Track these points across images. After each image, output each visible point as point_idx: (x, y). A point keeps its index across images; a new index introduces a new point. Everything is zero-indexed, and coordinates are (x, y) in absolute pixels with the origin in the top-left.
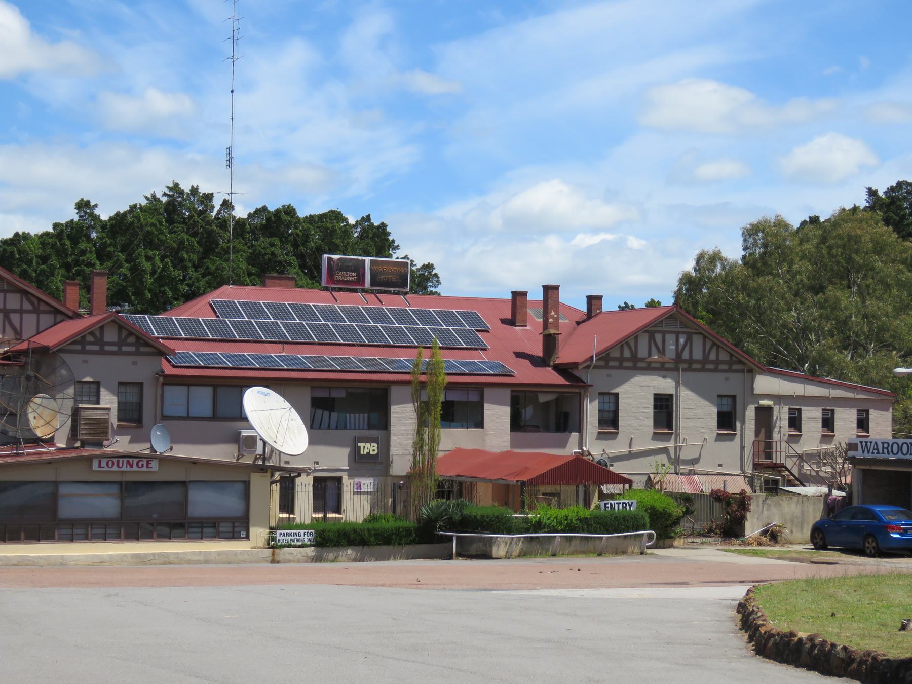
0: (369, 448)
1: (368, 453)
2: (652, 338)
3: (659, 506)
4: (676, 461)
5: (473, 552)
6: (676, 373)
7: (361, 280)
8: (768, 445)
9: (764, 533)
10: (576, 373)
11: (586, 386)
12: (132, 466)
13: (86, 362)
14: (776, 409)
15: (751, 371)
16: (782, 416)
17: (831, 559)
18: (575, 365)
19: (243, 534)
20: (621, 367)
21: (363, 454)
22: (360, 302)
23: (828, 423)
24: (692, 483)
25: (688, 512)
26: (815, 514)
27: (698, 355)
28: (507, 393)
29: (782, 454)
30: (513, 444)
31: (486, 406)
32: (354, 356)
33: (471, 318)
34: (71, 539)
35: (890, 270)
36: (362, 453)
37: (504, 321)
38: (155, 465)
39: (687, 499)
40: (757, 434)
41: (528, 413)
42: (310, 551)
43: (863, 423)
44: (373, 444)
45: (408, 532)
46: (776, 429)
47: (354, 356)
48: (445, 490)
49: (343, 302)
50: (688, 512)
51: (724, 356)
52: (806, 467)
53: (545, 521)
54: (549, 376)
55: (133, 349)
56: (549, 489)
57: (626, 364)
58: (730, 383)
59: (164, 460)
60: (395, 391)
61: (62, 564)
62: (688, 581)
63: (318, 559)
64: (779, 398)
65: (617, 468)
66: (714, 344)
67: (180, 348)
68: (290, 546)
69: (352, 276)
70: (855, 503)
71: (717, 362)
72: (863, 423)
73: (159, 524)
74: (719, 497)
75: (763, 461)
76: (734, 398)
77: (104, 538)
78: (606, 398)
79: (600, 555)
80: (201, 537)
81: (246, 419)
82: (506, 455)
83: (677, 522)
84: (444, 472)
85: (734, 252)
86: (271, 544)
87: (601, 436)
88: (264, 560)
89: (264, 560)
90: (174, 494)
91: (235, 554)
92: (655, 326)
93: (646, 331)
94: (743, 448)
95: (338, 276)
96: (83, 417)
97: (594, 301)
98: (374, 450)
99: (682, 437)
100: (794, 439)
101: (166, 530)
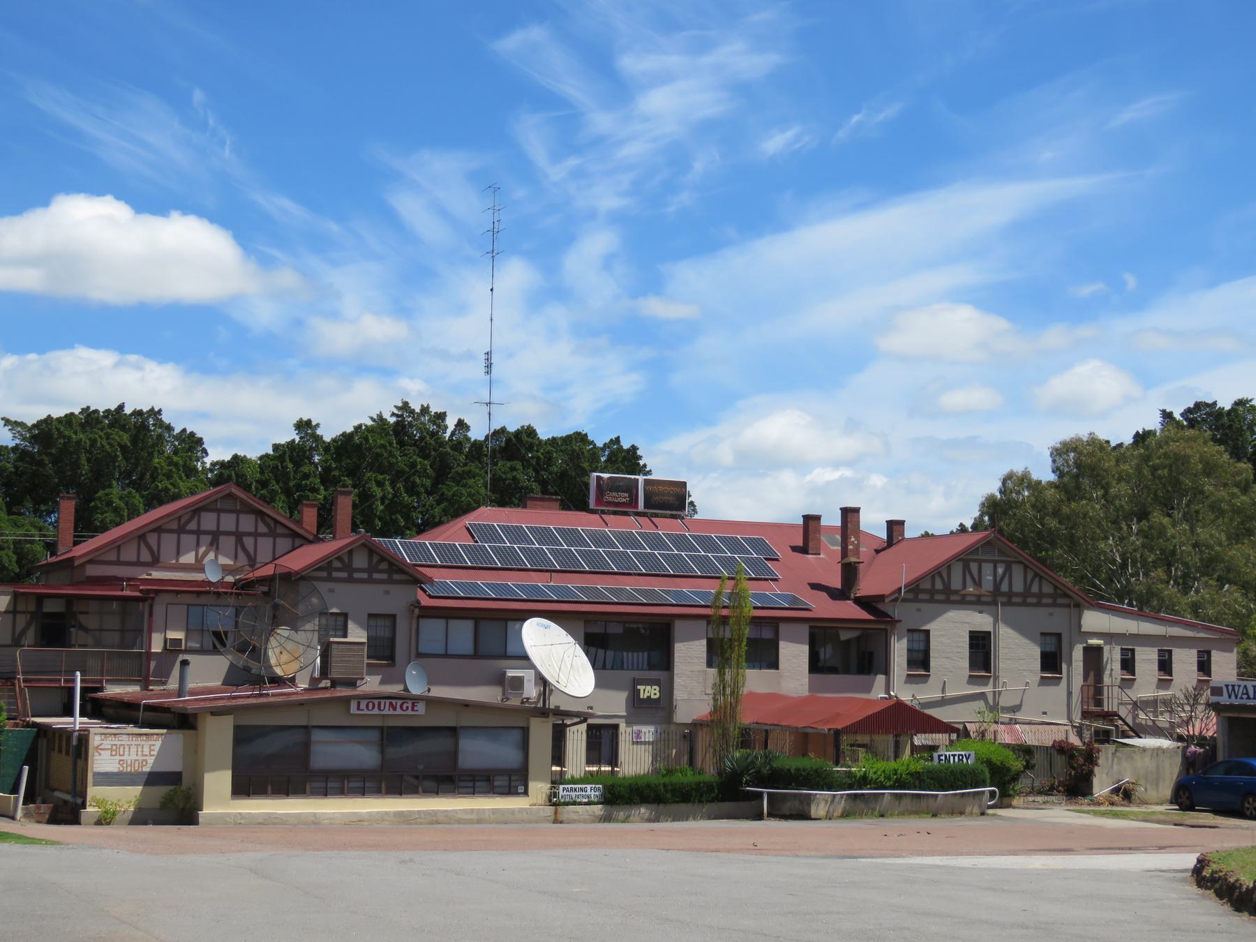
0: (649, 691)
1: (649, 697)
2: (966, 568)
3: (996, 759)
4: (994, 708)
5: (786, 811)
6: (993, 608)
7: (633, 501)
8: (1098, 691)
9: (1116, 791)
10: (881, 606)
11: (894, 622)
12: (395, 709)
14: (1106, 649)
15: (1078, 605)
16: (1112, 657)
17: (1201, 822)
18: (881, 598)
19: (521, 789)
20: (932, 601)
21: (643, 699)
22: (633, 526)
23: (1165, 665)
24: (1012, 732)
25: (1028, 766)
26: (1172, 771)
27: (1018, 586)
28: (804, 630)
29: (1114, 700)
30: (813, 687)
31: (782, 644)
32: (629, 585)
33: (758, 545)
34: (325, 793)
35: (1223, 493)
36: (641, 697)
37: (795, 549)
38: (421, 708)
39: (1026, 751)
40: (1086, 678)
41: (826, 653)
42: (598, 810)
43: (1204, 666)
44: (654, 687)
45: (710, 787)
46: (1107, 673)
47: (629, 585)
48: (746, 738)
49: (615, 526)
50: (1028, 766)
51: (1047, 589)
52: (1142, 716)
53: (871, 775)
54: (849, 610)
55: (384, 576)
56: (861, 739)
57: (937, 597)
58: (1054, 620)
59: (432, 702)
60: (679, 627)
61: (314, 822)
62: (1071, 847)
63: (607, 819)
64: (1109, 637)
65: (943, 714)
66: (1036, 575)
67: (438, 576)
68: (574, 803)
69: (623, 497)
70: (1220, 758)
71: (1040, 595)
72: (1204, 666)
73: (426, 777)
74: (1062, 749)
75: (1093, 708)
76: (1059, 636)
77: (362, 792)
78: (916, 636)
79: (934, 815)
80: (473, 792)
81: (526, 658)
82: (802, 701)
83: (1015, 778)
84: (746, 718)
85: (1044, 473)
86: (553, 801)
87: (910, 679)
88: (546, 820)
89: (546, 820)
90: (440, 744)
91: (512, 812)
92: (971, 553)
93: (959, 560)
94: (1070, 694)
95: (609, 497)
96: (335, 651)
97: (895, 526)
98: (655, 694)
99: (1001, 680)
100: (1127, 684)
101: (433, 784)
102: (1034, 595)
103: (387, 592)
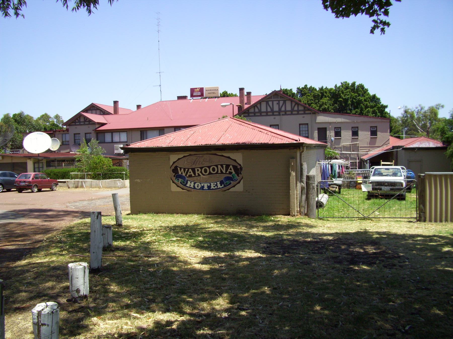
13: (76, 128)
27: (289, 108)
55: (88, 123)
57: (257, 114)
58: (306, 119)
71: (298, 111)
103: (89, 127)
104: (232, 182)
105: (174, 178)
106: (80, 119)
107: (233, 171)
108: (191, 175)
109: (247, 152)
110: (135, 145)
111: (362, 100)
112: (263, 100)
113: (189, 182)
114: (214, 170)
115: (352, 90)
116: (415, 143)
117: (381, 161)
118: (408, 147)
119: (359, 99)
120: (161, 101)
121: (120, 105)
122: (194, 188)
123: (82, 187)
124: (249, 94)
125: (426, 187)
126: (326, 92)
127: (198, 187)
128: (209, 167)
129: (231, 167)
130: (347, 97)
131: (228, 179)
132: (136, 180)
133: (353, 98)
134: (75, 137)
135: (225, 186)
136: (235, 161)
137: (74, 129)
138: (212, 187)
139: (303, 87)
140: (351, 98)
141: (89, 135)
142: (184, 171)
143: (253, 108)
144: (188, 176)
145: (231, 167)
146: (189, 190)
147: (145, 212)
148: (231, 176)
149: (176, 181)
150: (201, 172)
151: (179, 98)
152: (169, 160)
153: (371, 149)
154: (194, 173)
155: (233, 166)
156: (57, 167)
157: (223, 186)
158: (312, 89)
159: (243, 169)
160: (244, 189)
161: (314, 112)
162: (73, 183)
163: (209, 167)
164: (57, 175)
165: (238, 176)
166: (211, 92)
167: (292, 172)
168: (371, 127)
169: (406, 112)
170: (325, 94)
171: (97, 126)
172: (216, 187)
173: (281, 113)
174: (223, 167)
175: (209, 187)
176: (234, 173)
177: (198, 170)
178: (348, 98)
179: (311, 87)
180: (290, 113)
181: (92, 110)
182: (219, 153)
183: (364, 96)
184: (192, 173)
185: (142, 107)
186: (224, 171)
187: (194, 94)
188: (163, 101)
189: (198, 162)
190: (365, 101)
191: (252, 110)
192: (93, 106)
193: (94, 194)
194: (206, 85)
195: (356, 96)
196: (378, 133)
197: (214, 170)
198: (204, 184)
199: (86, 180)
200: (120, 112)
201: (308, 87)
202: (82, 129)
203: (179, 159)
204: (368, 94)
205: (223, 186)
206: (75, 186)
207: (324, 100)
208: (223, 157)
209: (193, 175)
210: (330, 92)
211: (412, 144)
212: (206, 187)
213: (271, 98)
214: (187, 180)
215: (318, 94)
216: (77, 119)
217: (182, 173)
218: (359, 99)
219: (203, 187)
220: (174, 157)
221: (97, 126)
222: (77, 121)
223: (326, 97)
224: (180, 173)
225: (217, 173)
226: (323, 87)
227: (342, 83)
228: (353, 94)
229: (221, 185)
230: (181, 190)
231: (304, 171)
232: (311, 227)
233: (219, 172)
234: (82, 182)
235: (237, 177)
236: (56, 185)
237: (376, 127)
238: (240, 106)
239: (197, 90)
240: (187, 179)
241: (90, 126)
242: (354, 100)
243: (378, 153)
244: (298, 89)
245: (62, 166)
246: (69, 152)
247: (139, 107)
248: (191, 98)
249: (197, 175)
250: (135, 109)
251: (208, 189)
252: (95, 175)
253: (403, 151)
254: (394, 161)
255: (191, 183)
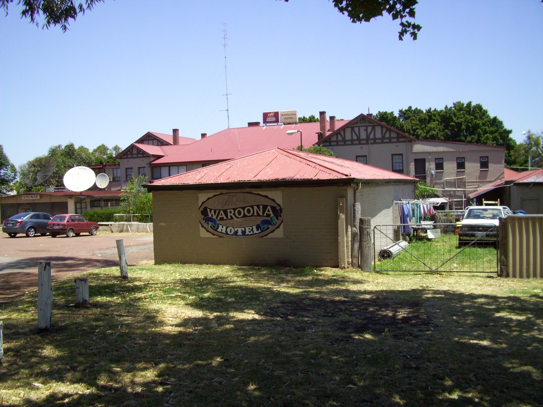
13: (128, 161)
27: (379, 135)
51: (393, 135)
55: (141, 155)
57: (340, 143)
58: (400, 148)
71: (390, 138)
93: (348, 127)
102: (387, 138)
104: (270, 226)
105: (203, 222)
106: (132, 151)
107: (271, 213)
108: (223, 218)
109: (287, 190)
110: (159, 182)
111: (479, 124)
112: (348, 126)
113: (220, 227)
114: (249, 211)
115: (467, 111)
116: (531, 177)
117: (483, 199)
118: (521, 182)
119: (476, 122)
120: (229, 129)
121: (181, 134)
122: (227, 233)
123: (127, 231)
124: (332, 118)
125: (509, 233)
126: (435, 115)
127: (231, 232)
128: (243, 208)
129: (269, 208)
130: (460, 120)
131: (265, 222)
132: (160, 224)
133: (468, 122)
134: (126, 172)
135: (262, 231)
136: (273, 200)
137: (125, 163)
138: (247, 233)
139: (407, 109)
140: (465, 122)
141: (143, 169)
142: (215, 212)
143: (335, 136)
144: (219, 219)
145: (269, 208)
146: (221, 235)
147: (170, 262)
148: (269, 219)
149: (205, 225)
150: (234, 214)
151: (250, 124)
152: (198, 200)
153: (480, 185)
154: (226, 215)
155: (272, 207)
156: (104, 208)
157: (260, 231)
158: (418, 112)
159: (284, 210)
160: (284, 235)
161: (409, 139)
162: (117, 226)
163: (243, 208)
164: (101, 217)
165: (278, 219)
166: (288, 116)
167: (341, 214)
168: (481, 157)
169: (529, 138)
170: (433, 117)
171: (152, 159)
172: (252, 233)
173: (370, 142)
174: (259, 209)
175: (244, 233)
176: (272, 215)
177: (231, 212)
178: (462, 121)
179: (416, 109)
180: (380, 141)
181: (148, 140)
182: (255, 191)
183: (483, 119)
184: (224, 216)
185: (207, 135)
186: (261, 214)
187: (268, 120)
188: (231, 129)
189: (231, 202)
190: (484, 124)
191: (334, 138)
192: (150, 136)
193: (137, 239)
194: (282, 109)
195: (472, 119)
196: (490, 165)
197: (249, 211)
198: (238, 229)
199: (132, 223)
200: (181, 142)
201: (413, 108)
202: (135, 163)
203: (209, 199)
204: (488, 116)
205: (260, 231)
206: (120, 230)
207: (433, 125)
208: (259, 196)
209: (225, 218)
210: (439, 115)
211: (526, 179)
212: (240, 233)
213: (357, 123)
214: (218, 224)
215: (425, 118)
216: (129, 151)
217: (212, 216)
218: (476, 122)
219: (236, 232)
220: (203, 197)
221: (152, 159)
222: (129, 153)
223: (434, 121)
224: (210, 216)
225: (253, 215)
226: (430, 109)
227: (454, 104)
228: (468, 116)
229: (258, 230)
230: (211, 236)
231: (356, 212)
232: (356, 282)
233: (255, 214)
234: (127, 225)
235: (276, 221)
236: (97, 228)
237: (487, 157)
238: (320, 133)
239: (271, 114)
240: (218, 222)
241: (144, 159)
242: (469, 124)
243: (488, 189)
244: (401, 111)
245: (108, 206)
246: (120, 190)
247: (203, 135)
248: (264, 125)
249: (229, 217)
250: (199, 138)
251: (243, 235)
252: (142, 217)
253: (515, 187)
254: (499, 200)
255: (223, 227)
